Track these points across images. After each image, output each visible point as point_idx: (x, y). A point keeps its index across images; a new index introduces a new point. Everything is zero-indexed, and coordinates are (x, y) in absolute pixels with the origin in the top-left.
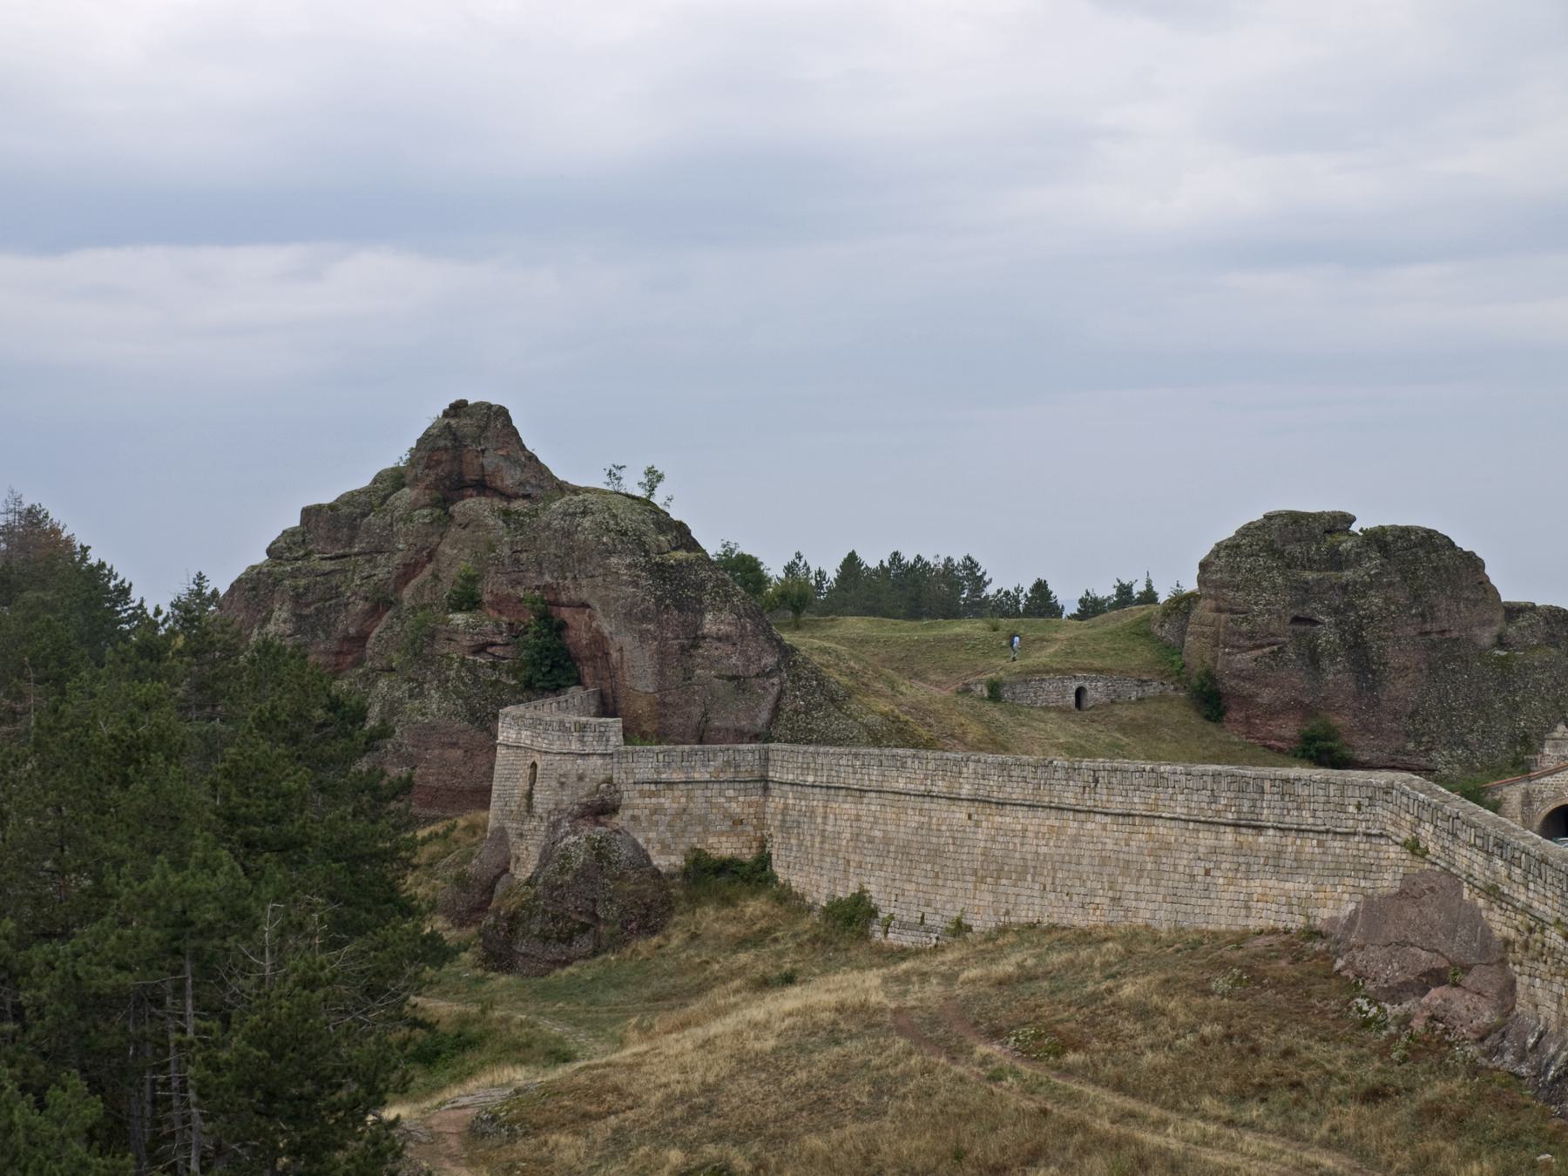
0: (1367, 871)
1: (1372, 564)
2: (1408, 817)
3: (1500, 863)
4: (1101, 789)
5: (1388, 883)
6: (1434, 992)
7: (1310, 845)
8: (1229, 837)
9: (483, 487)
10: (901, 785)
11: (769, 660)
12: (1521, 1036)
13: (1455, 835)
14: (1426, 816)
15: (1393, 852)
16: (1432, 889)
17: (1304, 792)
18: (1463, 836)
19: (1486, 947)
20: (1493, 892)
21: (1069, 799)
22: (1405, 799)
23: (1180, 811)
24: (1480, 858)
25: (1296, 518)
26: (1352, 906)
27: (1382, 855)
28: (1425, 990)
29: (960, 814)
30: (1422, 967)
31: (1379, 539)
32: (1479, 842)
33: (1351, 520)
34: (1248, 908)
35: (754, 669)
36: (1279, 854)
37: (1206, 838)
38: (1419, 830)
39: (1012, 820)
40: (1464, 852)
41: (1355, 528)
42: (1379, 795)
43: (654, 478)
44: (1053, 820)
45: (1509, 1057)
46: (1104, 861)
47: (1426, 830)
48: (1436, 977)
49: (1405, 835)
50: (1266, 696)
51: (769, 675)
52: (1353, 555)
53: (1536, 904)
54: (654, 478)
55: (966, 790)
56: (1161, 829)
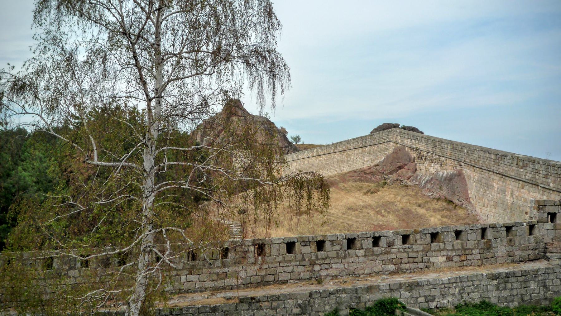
0: (386, 150)
4: (338, 147)
5: (391, 151)
6: (399, 171)
7: (376, 148)
8: (360, 150)
9: (235, 114)
10: (304, 157)
11: (287, 145)
12: (417, 177)
14: (399, 135)
15: (392, 144)
16: (400, 150)
18: (406, 137)
21: (332, 151)
23: (352, 147)
24: (409, 141)
25: (389, 124)
26: (383, 158)
28: (398, 171)
29: (313, 159)
30: (397, 166)
33: (399, 125)
34: (364, 164)
35: (284, 146)
37: (356, 152)
41: (400, 126)
42: (389, 133)
43: (267, 113)
44: (328, 156)
46: (338, 161)
48: (400, 168)
49: (394, 140)
51: (286, 147)
54: (267, 113)
55: (315, 155)
56: (348, 152)
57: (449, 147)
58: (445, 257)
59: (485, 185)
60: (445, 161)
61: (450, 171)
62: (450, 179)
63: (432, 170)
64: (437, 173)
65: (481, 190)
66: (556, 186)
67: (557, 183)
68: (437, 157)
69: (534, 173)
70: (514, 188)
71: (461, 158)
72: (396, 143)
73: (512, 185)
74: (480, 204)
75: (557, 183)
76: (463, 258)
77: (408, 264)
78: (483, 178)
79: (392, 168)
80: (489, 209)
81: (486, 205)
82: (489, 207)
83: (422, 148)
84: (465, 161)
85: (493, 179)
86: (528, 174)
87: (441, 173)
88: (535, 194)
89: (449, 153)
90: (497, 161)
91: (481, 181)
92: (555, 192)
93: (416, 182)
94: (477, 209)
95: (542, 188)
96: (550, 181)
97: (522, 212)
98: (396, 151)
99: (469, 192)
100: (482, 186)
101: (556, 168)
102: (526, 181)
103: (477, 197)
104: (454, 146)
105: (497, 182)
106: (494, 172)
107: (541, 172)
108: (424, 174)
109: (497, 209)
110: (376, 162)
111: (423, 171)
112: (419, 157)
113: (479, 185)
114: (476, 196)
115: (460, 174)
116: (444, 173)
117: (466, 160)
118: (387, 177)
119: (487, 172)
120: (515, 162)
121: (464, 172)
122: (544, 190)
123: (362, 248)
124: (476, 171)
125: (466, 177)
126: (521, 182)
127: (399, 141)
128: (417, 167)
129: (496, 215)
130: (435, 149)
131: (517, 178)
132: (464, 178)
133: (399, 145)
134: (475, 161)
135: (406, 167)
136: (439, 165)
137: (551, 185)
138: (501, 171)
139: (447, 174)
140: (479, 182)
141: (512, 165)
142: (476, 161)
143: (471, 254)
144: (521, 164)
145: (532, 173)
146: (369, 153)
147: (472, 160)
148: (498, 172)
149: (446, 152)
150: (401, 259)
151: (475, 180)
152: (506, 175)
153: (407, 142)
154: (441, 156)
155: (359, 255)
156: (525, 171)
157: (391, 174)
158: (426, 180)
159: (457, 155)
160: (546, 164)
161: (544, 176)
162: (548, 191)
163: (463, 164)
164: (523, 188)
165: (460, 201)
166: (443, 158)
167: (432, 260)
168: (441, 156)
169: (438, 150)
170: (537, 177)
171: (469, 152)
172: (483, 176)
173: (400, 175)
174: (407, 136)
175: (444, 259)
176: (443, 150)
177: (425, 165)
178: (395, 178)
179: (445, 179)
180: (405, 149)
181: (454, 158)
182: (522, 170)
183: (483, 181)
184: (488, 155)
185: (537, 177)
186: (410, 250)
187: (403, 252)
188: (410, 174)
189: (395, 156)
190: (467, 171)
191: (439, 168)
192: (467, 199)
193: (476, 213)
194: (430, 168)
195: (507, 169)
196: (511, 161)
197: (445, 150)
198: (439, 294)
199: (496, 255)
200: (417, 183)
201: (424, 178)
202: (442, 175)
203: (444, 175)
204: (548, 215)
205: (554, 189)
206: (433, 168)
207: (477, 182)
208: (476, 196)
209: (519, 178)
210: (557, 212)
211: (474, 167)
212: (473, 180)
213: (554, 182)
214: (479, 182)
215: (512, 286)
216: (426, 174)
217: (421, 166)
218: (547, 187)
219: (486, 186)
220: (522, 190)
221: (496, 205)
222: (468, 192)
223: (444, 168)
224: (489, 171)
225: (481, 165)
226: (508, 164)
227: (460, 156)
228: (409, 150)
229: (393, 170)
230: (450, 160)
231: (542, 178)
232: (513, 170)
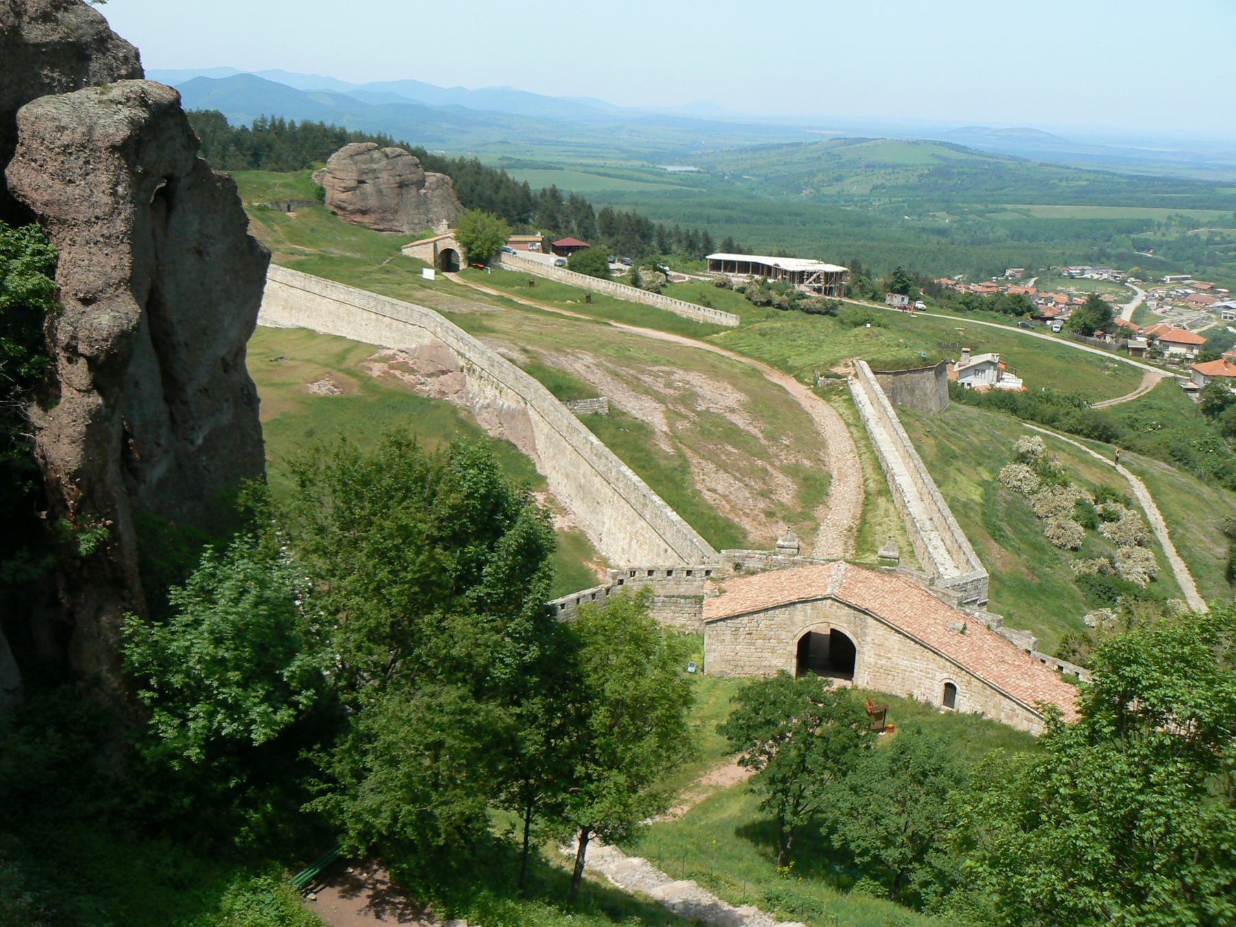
0: (420, 337)
6: (442, 378)
8: (374, 316)
12: (468, 393)
17: (397, 307)
36: (391, 324)
37: (366, 314)
39: (294, 291)
47: (438, 329)
48: (444, 372)
49: (432, 330)
50: (350, 208)
72: (434, 333)
73: (585, 467)
87: (501, 403)
93: (467, 401)
98: (435, 347)
110: (403, 347)
115: (525, 413)
120: (589, 444)
127: (440, 335)
139: (509, 407)
146: (389, 326)
153: (451, 340)
174: (451, 333)
178: (437, 387)
179: (507, 413)
188: (458, 387)
189: (434, 352)
191: (498, 394)
192: (534, 449)
214: (547, 436)
217: (473, 384)
221: (567, 476)
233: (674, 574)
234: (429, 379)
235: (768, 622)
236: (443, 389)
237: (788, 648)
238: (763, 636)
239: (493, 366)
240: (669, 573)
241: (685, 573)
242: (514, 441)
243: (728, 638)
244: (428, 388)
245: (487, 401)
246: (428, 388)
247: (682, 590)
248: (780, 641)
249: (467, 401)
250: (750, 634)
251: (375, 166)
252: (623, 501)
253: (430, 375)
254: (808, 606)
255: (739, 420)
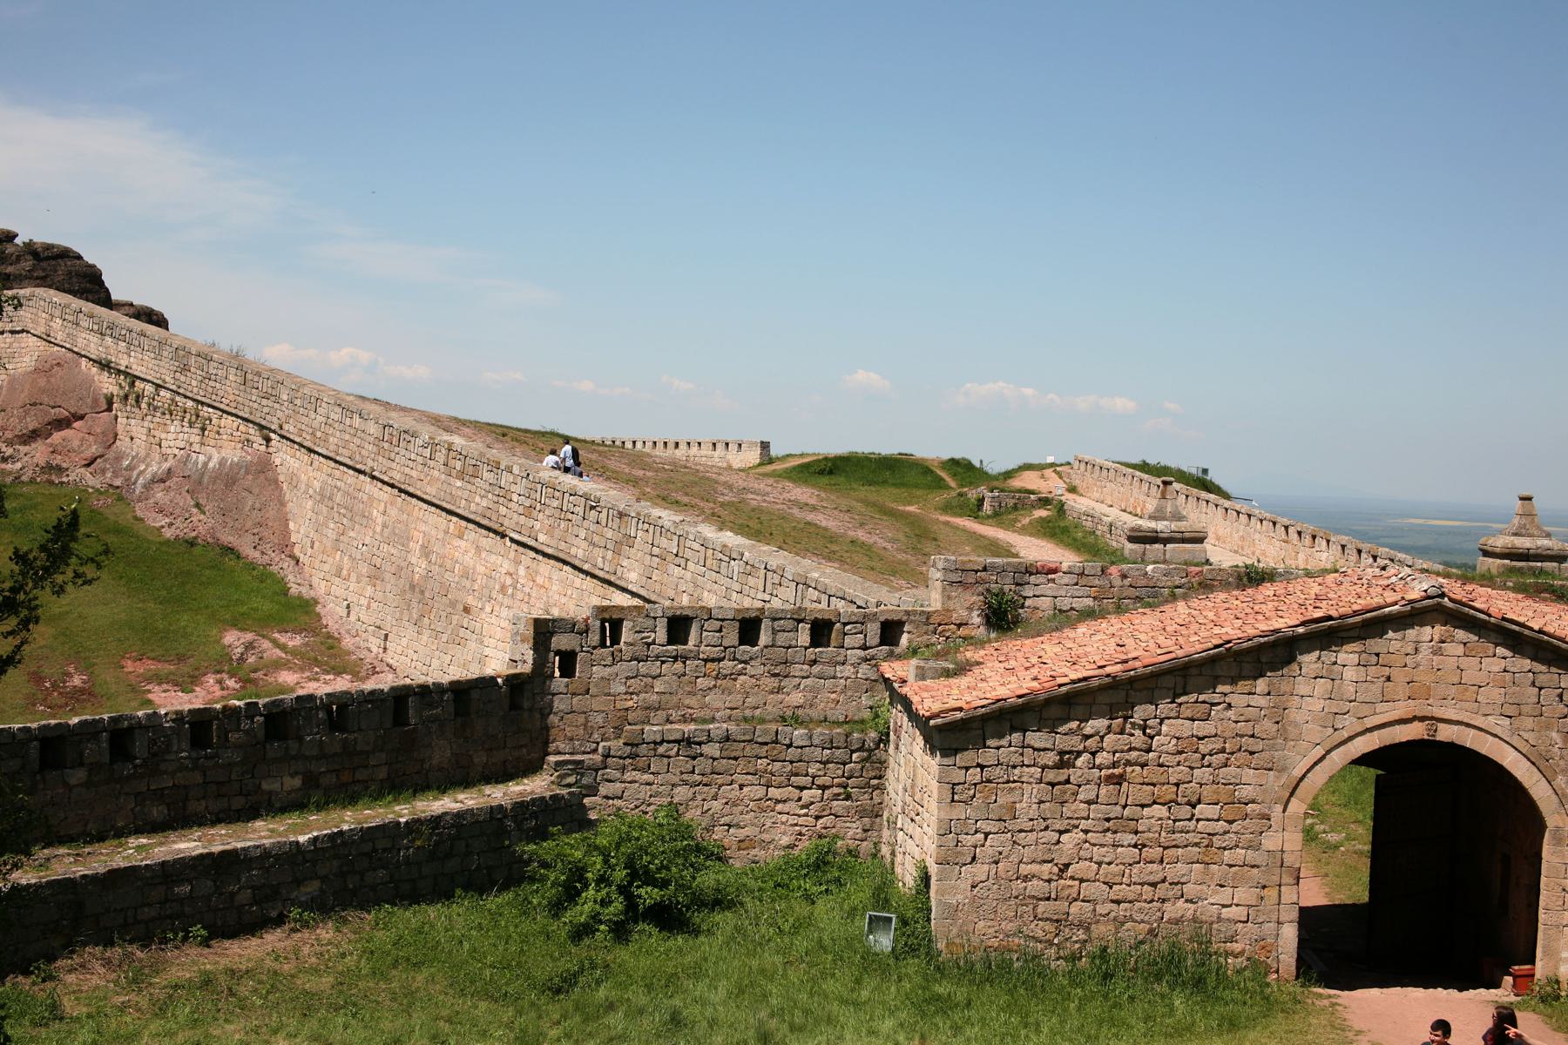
1: (27, 264)
2: (44, 315)
3: (110, 340)
5: (26, 363)
6: (57, 437)
12: (119, 458)
13: (77, 324)
14: (57, 313)
19: (96, 401)
20: (105, 366)
22: (42, 303)
24: (95, 339)
27: (23, 345)
31: (31, 250)
32: (96, 327)
38: (52, 324)
40: (84, 335)
41: (18, 241)
45: (109, 475)
48: (62, 424)
49: (40, 330)
52: (14, 257)
53: (134, 367)
57: (231, 377)
58: (301, 777)
59: (342, 511)
60: (214, 421)
61: (232, 453)
62: (229, 478)
63: (172, 444)
64: (189, 455)
65: (332, 526)
66: (553, 543)
67: (557, 533)
68: (190, 404)
69: (496, 499)
70: (434, 532)
71: (268, 417)
74: (326, 567)
75: (557, 533)
76: (346, 777)
77: (203, 803)
78: (339, 490)
79: (32, 424)
80: (353, 586)
81: (345, 572)
82: (353, 577)
83: (137, 370)
84: (281, 428)
85: (371, 497)
86: (478, 499)
87: (202, 458)
88: (494, 557)
89: (232, 397)
90: (386, 445)
91: (330, 498)
92: (552, 562)
93: (116, 474)
94: (315, 581)
95: (514, 546)
96: (538, 526)
97: (453, 604)
98: (44, 369)
99: (292, 525)
100: (336, 515)
101: (557, 494)
102: (472, 517)
103: (317, 544)
104: (249, 377)
105: (381, 508)
106: (373, 477)
107: (515, 497)
108: (142, 454)
109: (378, 588)
111: (140, 446)
112: (126, 397)
113: (325, 509)
114: (313, 543)
115: (264, 467)
116: (210, 459)
117: (286, 427)
118: (9, 451)
119: (351, 472)
120: (441, 456)
121: (278, 462)
122: (521, 549)
123: (81, 764)
124: (316, 463)
125: (281, 478)
126: (455, 519)
127: (60, 337)
128: (120, 428)
129: (374, 605)
130: (183, 378)
131: (444, 505)
132: (276, 481)
133: (56, 348)
134: (313, 434)
135: (75, 425)
136: (196, 431)
137: (542, 538)
138: (398, 476)
139: (222, 462)
140: (324, 497)
141: (432, 463)
142: (319, 434)
143: (366, 767)
144: (458, 465)
145: (490, 495)
147: (303, 427)
148: (386, 479)
149: (221, 393)
150: (185, 787)
151: (311, 491)
152: (411, 490)
154: (203, 403)
155: (73, 781)
156: (469, 486)
157: (25, 443)
158: (148, 476)
159: (256, 405)
160: (531, 477)
161: (521, 510)
162: (532, 554)
163: (273, 436)
164: (461, 537)
165: (263, 553)
166: (211, 410)
167: (265, 786)
168: (203, 403)
169: (194, 383)
170: (503, 510)
171: (298, 402)
172: (339, 484)
173: (60, 448)
175: (297, 782)
176: (212, 383)
177: (146, 424)
179: (214, 480)
180: (78, 365)
181: (246, 416)
182: (459, 483)
183: (338, 498)
184: (357, 421)
185: (503, 510)
186: (211, 763)
187: (192, 770)
188: (94, 450)
189: (42, 382)
190: (286, 459)
192: (285, 547)
193: (312, 593)
194: (163, 436)
195: (414, 474)
196: (427, 453)
197: (218, 385)
198: (290, 879)
199: (426, 766)
200: (118, 483)
201: (142, 467)
202: (205, 464)
203: (211, 465)
204: (556, 655)
205: (549, 551)
206: (175, 436)
207: (318, 498)
208: (313, 543)
209: (448, 506)
210: (578, 649)
211: (310, 450)
212: (306, 492)
213: (549, 533)
214: (324, 497)
215: (467, 846)
216: (148, 455)
217: (134, 431)
218: (531, 543)
219: (349, 515)
220: (457, 542)
221: (375, 576)
222: (287, 525)
223: (212, 442)
224: (360, 471)
225: (332, 447)
226: (420, 459)
227: (266, 410)
228: (94, 370)
229: (34, 431)
230: (230, 417)
231: (515, 516)
232: (433, 480)
233: (764, 639)
234: (24, 449)
235: (1186, 728)
236: (57, 460)
237: (1270, 842)
238: (1168, 792)
239: (185, 369)
240: (749, 628)
241: (804, 637)
242: (227, 538)
243: (1028, 799)
244: (18, 465)
245: (166, 466)
246: (18, 465)
247: (796, 698)
248: (1234, 809)
249: (116, 474)
250: (1118, 780)
251: (10, 269)
252: (546, 566)
253: (32, 436)
254: (1347, 655)
255: (821, 519)
